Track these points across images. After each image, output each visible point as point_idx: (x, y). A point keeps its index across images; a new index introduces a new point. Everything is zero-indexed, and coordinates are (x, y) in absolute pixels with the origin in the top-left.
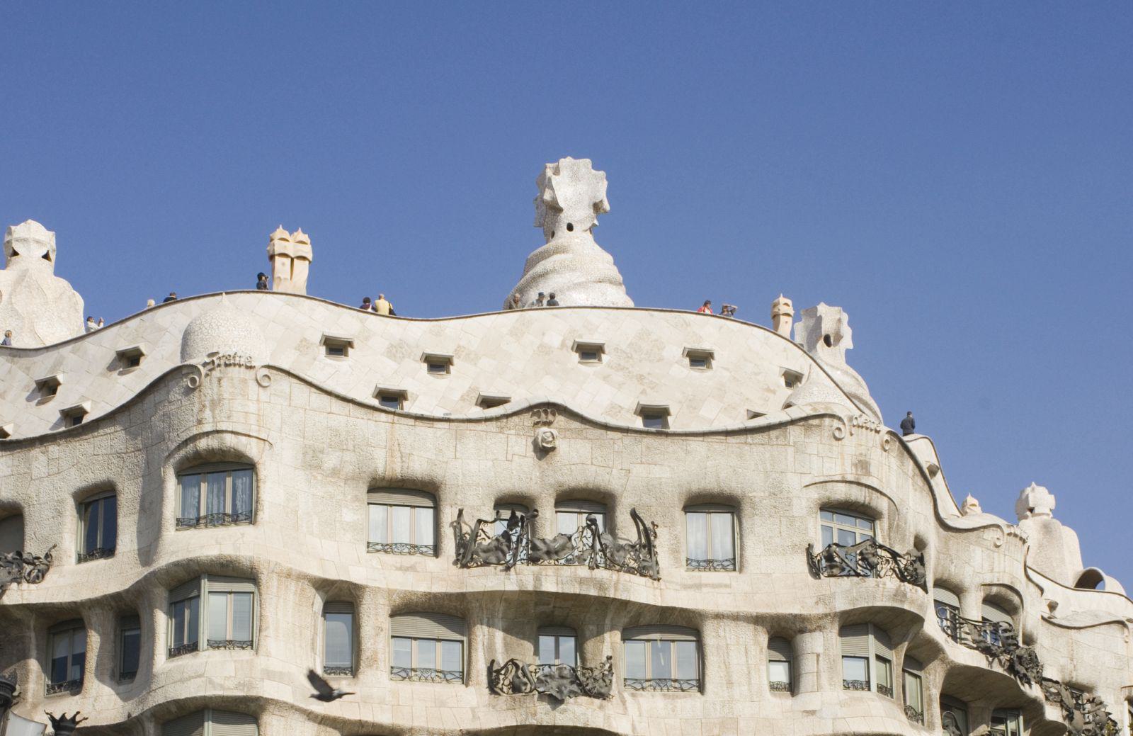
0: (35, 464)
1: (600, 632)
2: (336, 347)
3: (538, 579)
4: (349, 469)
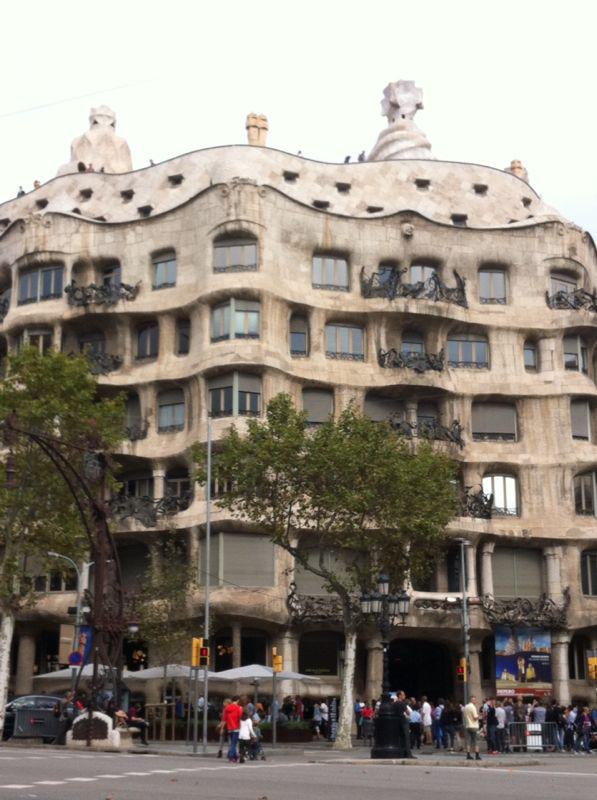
0: (128, 237)
1: (437, 332)
2: (290, 177)
3: (407, 307)
4: (304, 243)
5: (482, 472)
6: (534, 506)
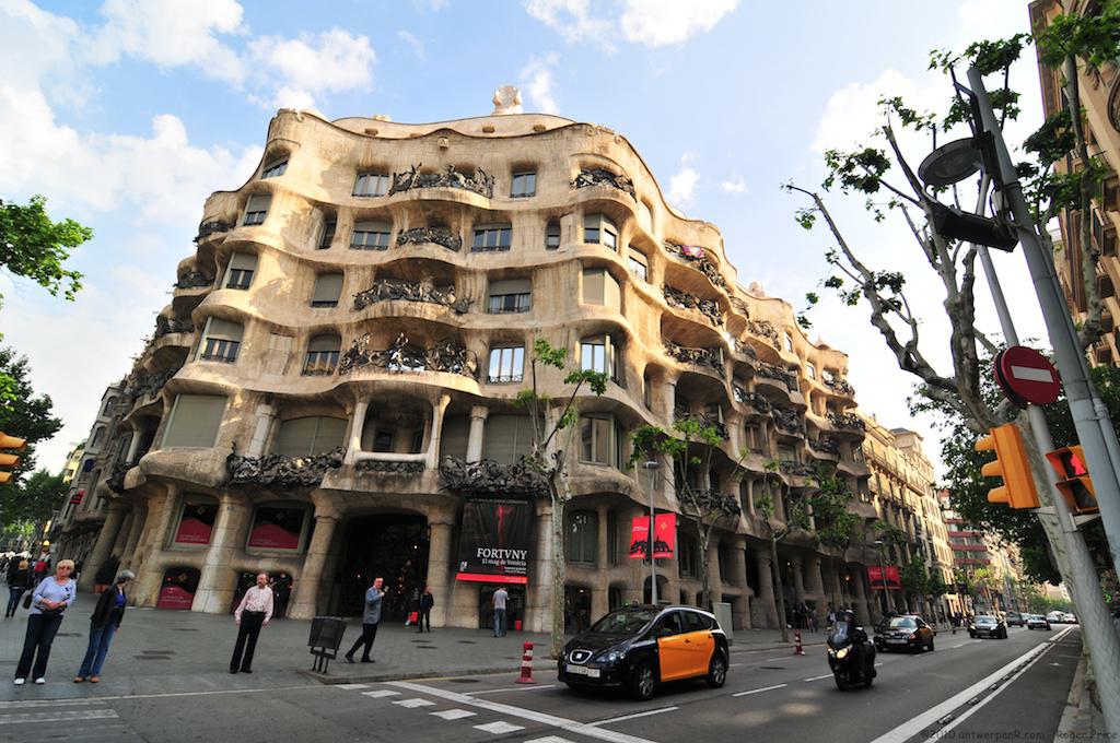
3: (420, 194)
4: (345, 161)
5: (486, 340)
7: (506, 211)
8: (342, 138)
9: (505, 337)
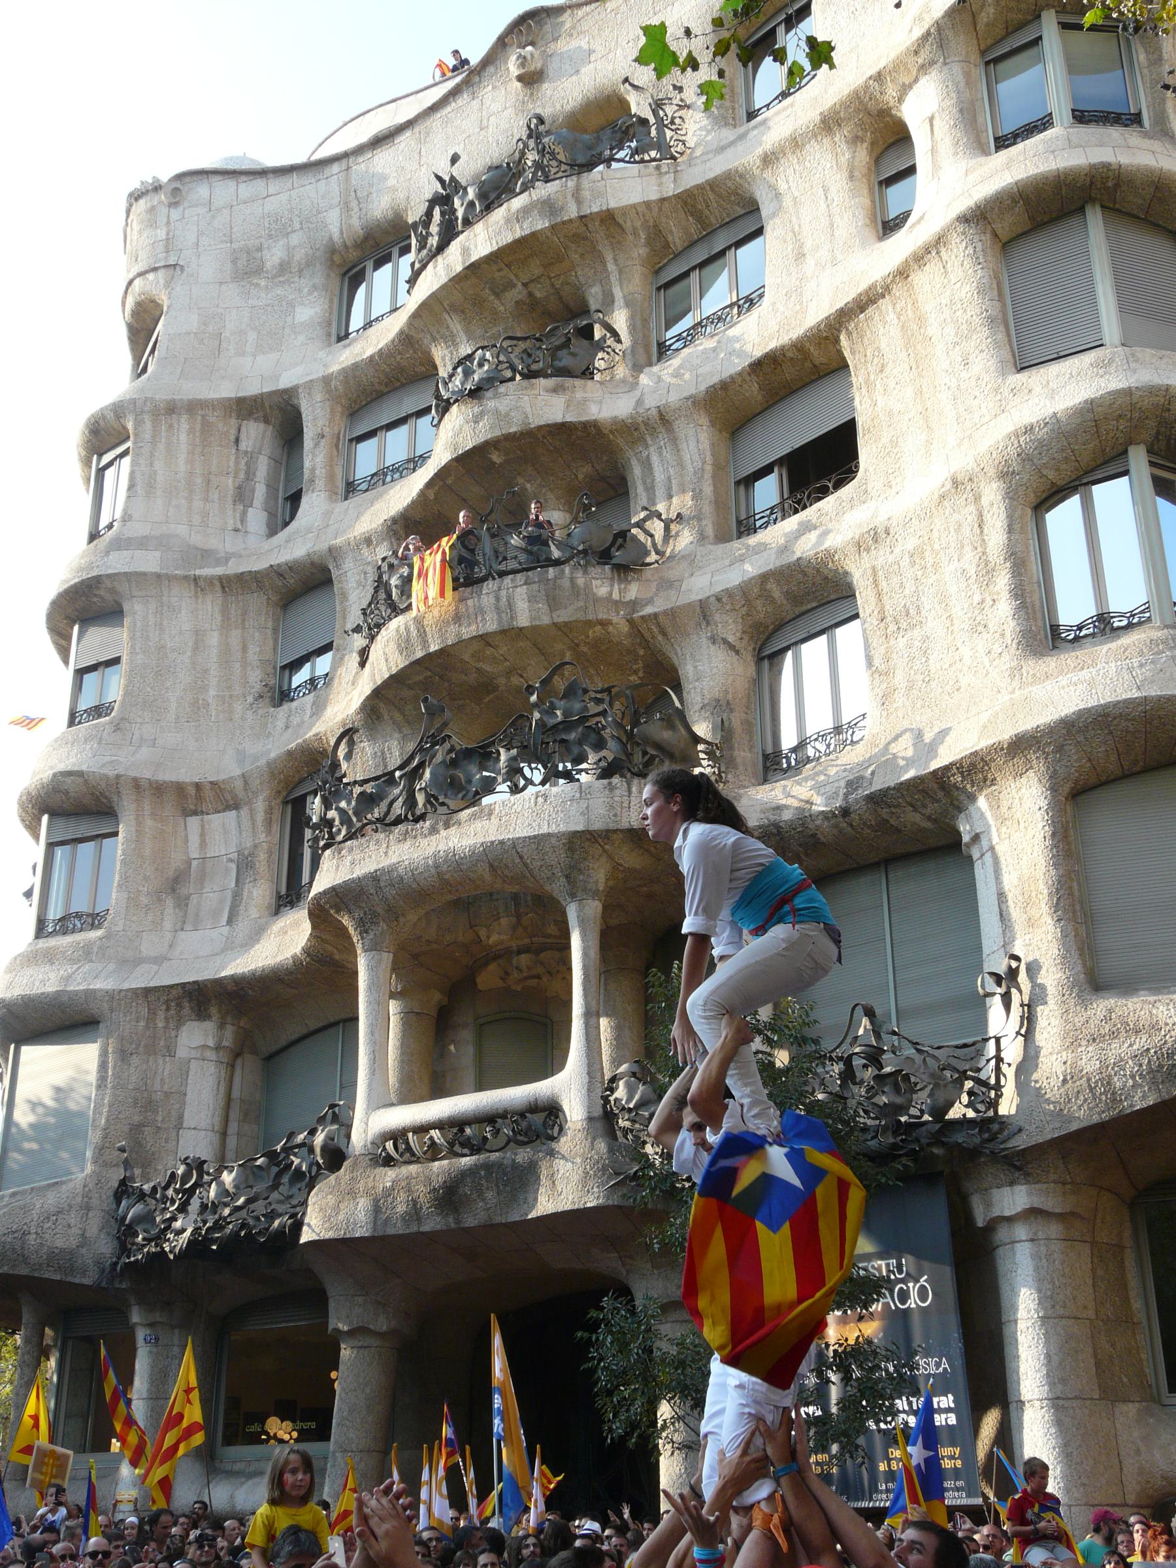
3: (465, 251)
4: (299, 255)
6: (899, 679)
7: (728, 175)
8: (280, 198)
9: (794, 598)
